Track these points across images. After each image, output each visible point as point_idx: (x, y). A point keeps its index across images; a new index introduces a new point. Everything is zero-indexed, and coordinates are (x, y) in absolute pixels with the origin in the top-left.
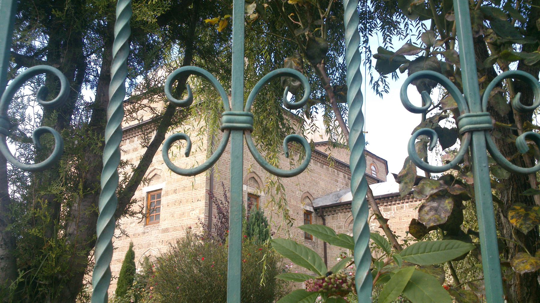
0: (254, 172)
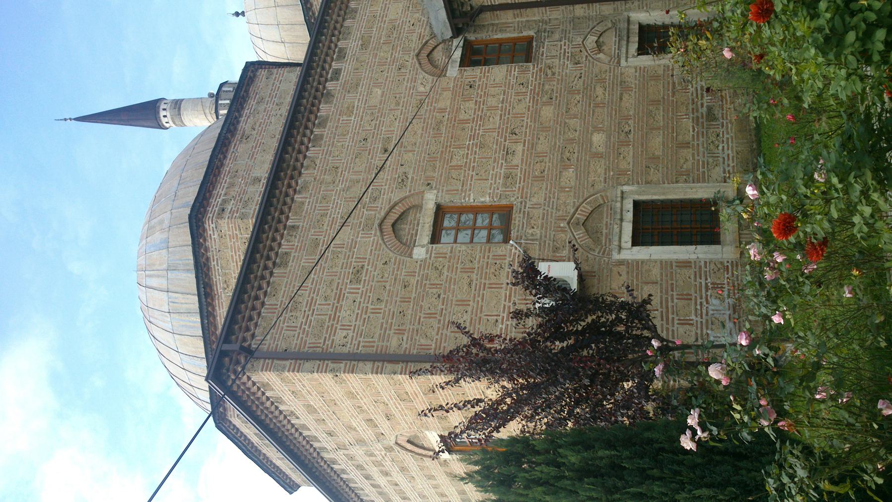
0: (380, 225)
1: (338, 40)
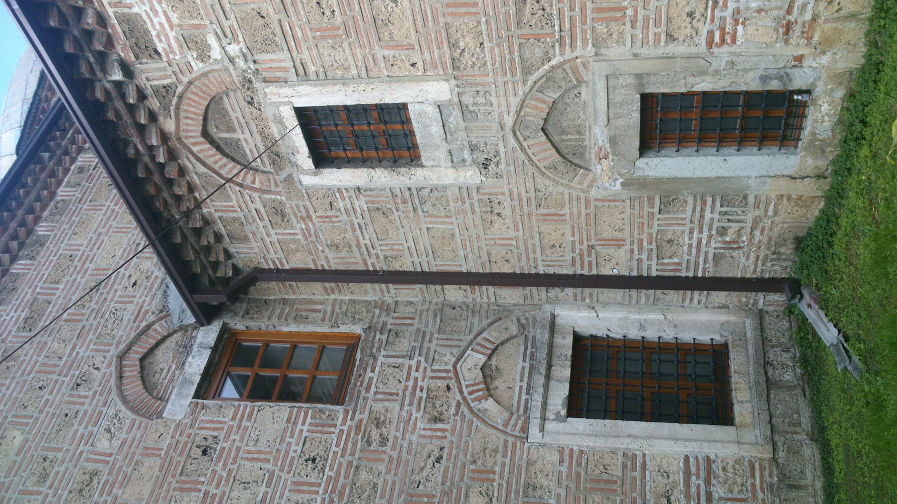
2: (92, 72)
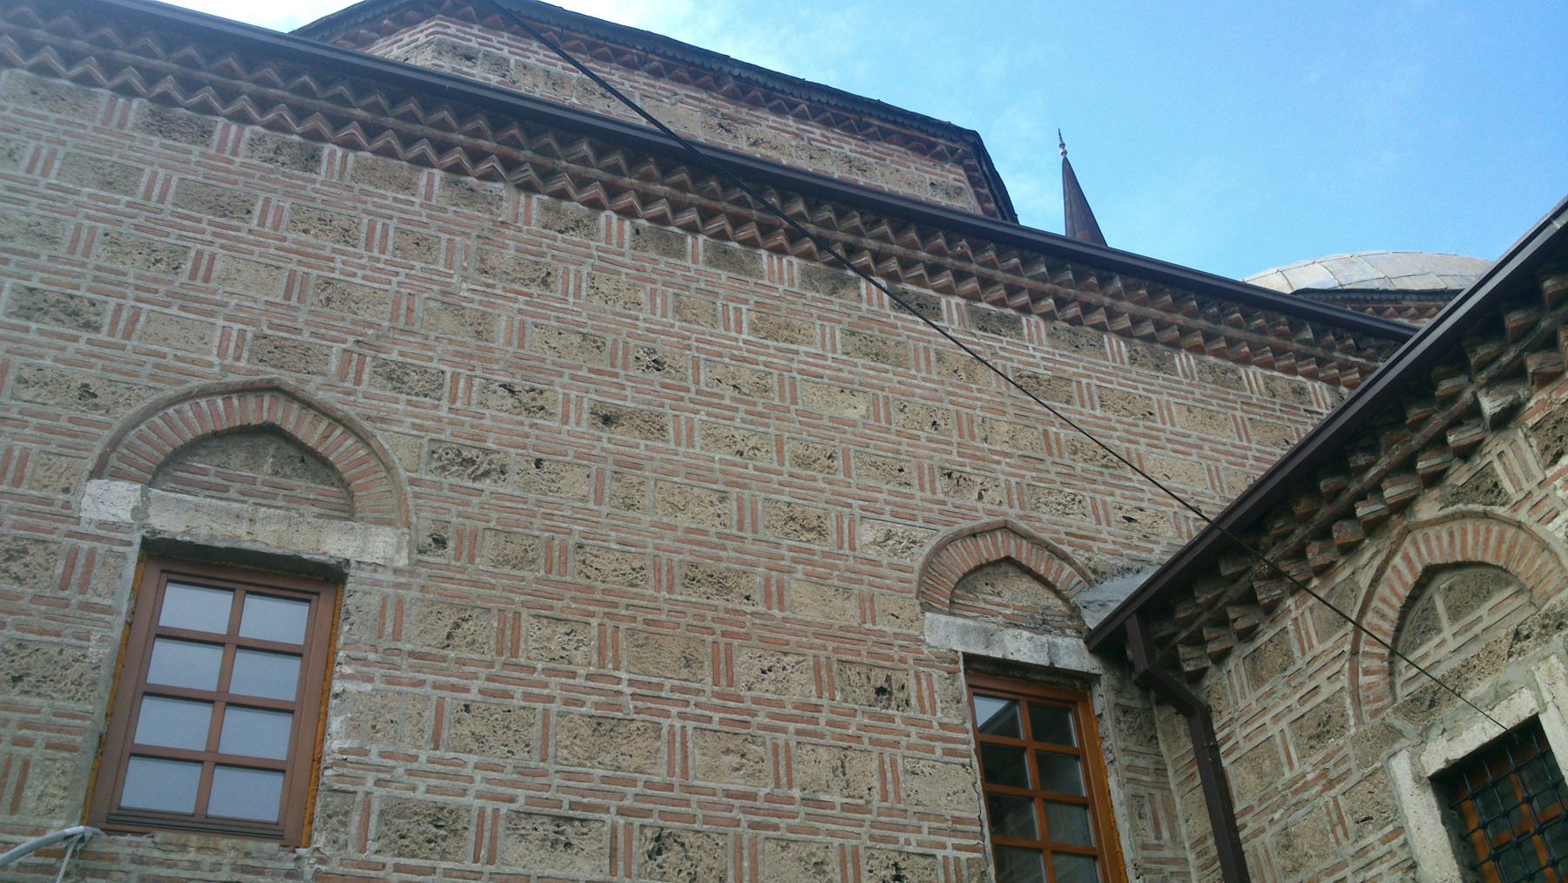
0: (273, 388)
1: (1048, 317)
2: (1482, 366)
